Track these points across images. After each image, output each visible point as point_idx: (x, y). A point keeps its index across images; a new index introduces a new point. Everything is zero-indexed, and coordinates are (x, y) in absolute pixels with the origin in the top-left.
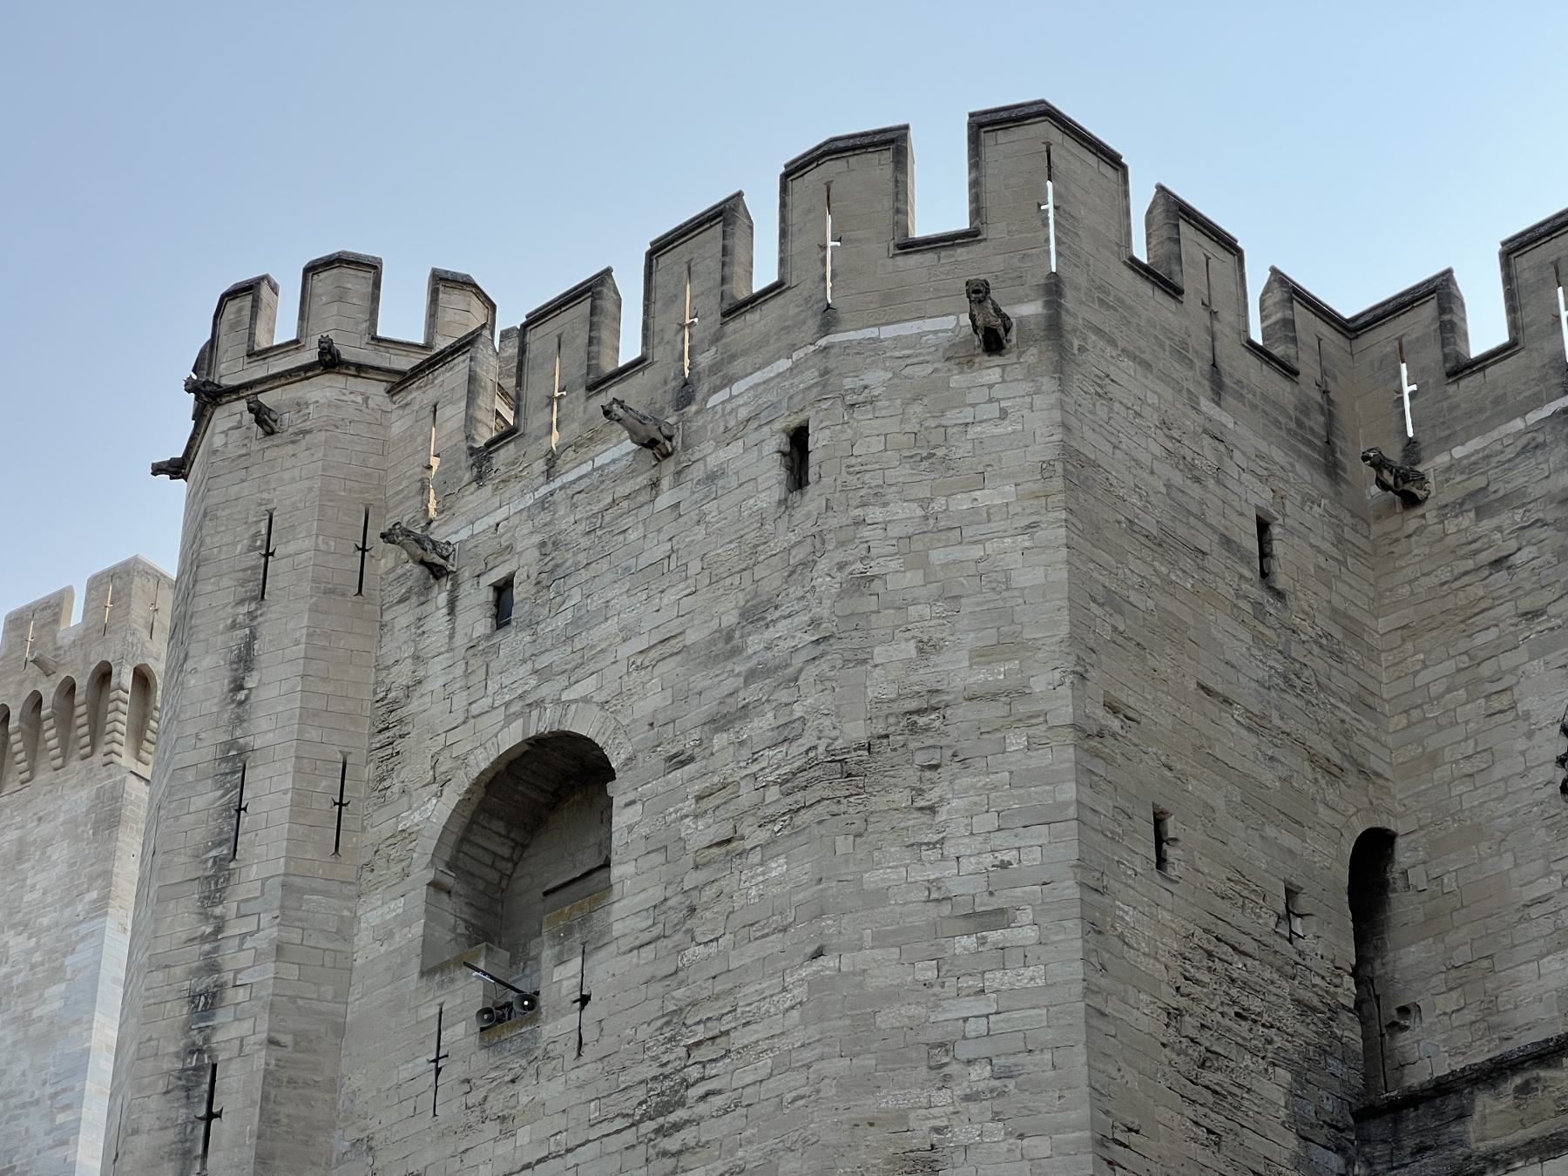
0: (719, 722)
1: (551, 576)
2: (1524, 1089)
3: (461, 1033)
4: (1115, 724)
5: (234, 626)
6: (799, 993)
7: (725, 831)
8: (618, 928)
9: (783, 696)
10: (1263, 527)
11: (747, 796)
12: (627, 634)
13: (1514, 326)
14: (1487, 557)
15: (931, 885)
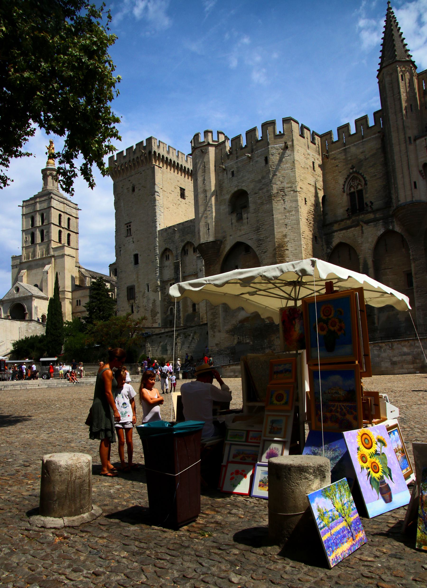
0: (261, 189)
1: (238, 171)
2: (339, 224)
3: (234, 221)
4: (301, 190)
5: (202, 176)
6: (271, 219)
7: (262, 201)
8: (251, 211)
9: (267, 187)
10: (313, 163)
11: (264, 198)
12: (248, 179)
13: (339, 138)
14: (335, 165)
15: (284, 208)
